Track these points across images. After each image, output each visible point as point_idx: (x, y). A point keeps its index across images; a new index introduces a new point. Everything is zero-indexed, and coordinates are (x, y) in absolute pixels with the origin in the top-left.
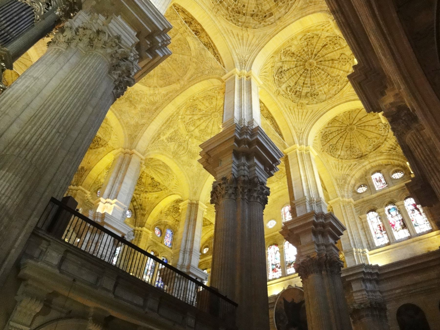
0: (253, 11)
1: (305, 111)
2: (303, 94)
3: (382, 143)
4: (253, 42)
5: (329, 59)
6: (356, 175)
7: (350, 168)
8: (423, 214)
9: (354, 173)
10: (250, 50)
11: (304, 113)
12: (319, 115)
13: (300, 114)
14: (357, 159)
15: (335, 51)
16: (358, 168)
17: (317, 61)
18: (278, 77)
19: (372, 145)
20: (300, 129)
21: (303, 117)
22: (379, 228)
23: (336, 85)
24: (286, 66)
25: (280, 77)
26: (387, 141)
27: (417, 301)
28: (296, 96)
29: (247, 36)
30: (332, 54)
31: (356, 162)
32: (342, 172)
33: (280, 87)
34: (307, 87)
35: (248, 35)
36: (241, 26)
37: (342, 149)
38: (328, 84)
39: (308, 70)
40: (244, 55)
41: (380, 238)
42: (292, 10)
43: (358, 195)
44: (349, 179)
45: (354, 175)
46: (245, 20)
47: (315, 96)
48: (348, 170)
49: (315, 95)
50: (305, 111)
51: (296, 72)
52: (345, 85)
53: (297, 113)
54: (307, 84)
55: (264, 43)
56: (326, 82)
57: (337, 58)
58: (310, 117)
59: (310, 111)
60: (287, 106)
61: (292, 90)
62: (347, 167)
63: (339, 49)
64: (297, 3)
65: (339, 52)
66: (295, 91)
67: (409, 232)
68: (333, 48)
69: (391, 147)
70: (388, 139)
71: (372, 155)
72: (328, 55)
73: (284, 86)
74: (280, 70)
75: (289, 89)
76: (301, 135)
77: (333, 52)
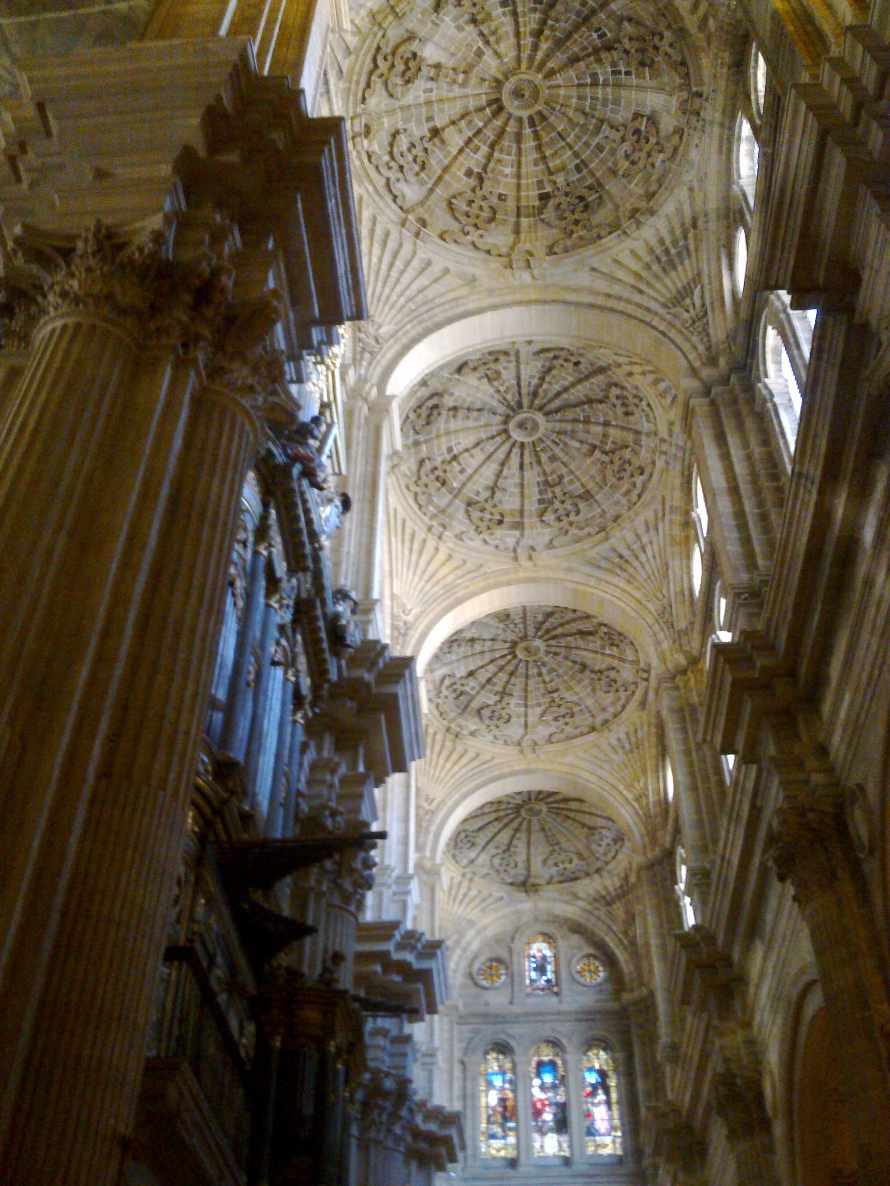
0: (478, 494)
2: (475, 705)
3: (588, 874)
4: (441, 574)
5: (578, 659)
7: (484, 905)
8: (615, 1107)
10: (426, 593)
11: (454, 757)
12: (488, 776)
13: (445, 753)
15: (603, 654)
21: (449, 765)
23: (562, 721)
26: (601, 876)
29: (432, 551)
30: (591, 655)
31: (503, 894)
32: (460, 912)
34: (491, 691)
36: (431, 518)
37: (484, 848)
38: (543, 707)
39: (515, 656)
40: (409, 607)
43: (478, 990)
45: (485, 928)
46: (449, 504)
47: (500, 723)
50: (460, 749)
52: (582, 734)
54: (495, 684)
55: (466, 591)
56: (541, 701)
57: (597, 668)
58: (464, 771)
59: (471, 754)
62: (477, 901)
63: (613, 657)
65: (609, 661)
67: (571, 1147)
68: (603, 647)
69: (604, 893)
70: (605, 873)
71: (550, 892)
72: (582, 653)
75: (447, 682)
76: (427, 817)
77: (596, 652)
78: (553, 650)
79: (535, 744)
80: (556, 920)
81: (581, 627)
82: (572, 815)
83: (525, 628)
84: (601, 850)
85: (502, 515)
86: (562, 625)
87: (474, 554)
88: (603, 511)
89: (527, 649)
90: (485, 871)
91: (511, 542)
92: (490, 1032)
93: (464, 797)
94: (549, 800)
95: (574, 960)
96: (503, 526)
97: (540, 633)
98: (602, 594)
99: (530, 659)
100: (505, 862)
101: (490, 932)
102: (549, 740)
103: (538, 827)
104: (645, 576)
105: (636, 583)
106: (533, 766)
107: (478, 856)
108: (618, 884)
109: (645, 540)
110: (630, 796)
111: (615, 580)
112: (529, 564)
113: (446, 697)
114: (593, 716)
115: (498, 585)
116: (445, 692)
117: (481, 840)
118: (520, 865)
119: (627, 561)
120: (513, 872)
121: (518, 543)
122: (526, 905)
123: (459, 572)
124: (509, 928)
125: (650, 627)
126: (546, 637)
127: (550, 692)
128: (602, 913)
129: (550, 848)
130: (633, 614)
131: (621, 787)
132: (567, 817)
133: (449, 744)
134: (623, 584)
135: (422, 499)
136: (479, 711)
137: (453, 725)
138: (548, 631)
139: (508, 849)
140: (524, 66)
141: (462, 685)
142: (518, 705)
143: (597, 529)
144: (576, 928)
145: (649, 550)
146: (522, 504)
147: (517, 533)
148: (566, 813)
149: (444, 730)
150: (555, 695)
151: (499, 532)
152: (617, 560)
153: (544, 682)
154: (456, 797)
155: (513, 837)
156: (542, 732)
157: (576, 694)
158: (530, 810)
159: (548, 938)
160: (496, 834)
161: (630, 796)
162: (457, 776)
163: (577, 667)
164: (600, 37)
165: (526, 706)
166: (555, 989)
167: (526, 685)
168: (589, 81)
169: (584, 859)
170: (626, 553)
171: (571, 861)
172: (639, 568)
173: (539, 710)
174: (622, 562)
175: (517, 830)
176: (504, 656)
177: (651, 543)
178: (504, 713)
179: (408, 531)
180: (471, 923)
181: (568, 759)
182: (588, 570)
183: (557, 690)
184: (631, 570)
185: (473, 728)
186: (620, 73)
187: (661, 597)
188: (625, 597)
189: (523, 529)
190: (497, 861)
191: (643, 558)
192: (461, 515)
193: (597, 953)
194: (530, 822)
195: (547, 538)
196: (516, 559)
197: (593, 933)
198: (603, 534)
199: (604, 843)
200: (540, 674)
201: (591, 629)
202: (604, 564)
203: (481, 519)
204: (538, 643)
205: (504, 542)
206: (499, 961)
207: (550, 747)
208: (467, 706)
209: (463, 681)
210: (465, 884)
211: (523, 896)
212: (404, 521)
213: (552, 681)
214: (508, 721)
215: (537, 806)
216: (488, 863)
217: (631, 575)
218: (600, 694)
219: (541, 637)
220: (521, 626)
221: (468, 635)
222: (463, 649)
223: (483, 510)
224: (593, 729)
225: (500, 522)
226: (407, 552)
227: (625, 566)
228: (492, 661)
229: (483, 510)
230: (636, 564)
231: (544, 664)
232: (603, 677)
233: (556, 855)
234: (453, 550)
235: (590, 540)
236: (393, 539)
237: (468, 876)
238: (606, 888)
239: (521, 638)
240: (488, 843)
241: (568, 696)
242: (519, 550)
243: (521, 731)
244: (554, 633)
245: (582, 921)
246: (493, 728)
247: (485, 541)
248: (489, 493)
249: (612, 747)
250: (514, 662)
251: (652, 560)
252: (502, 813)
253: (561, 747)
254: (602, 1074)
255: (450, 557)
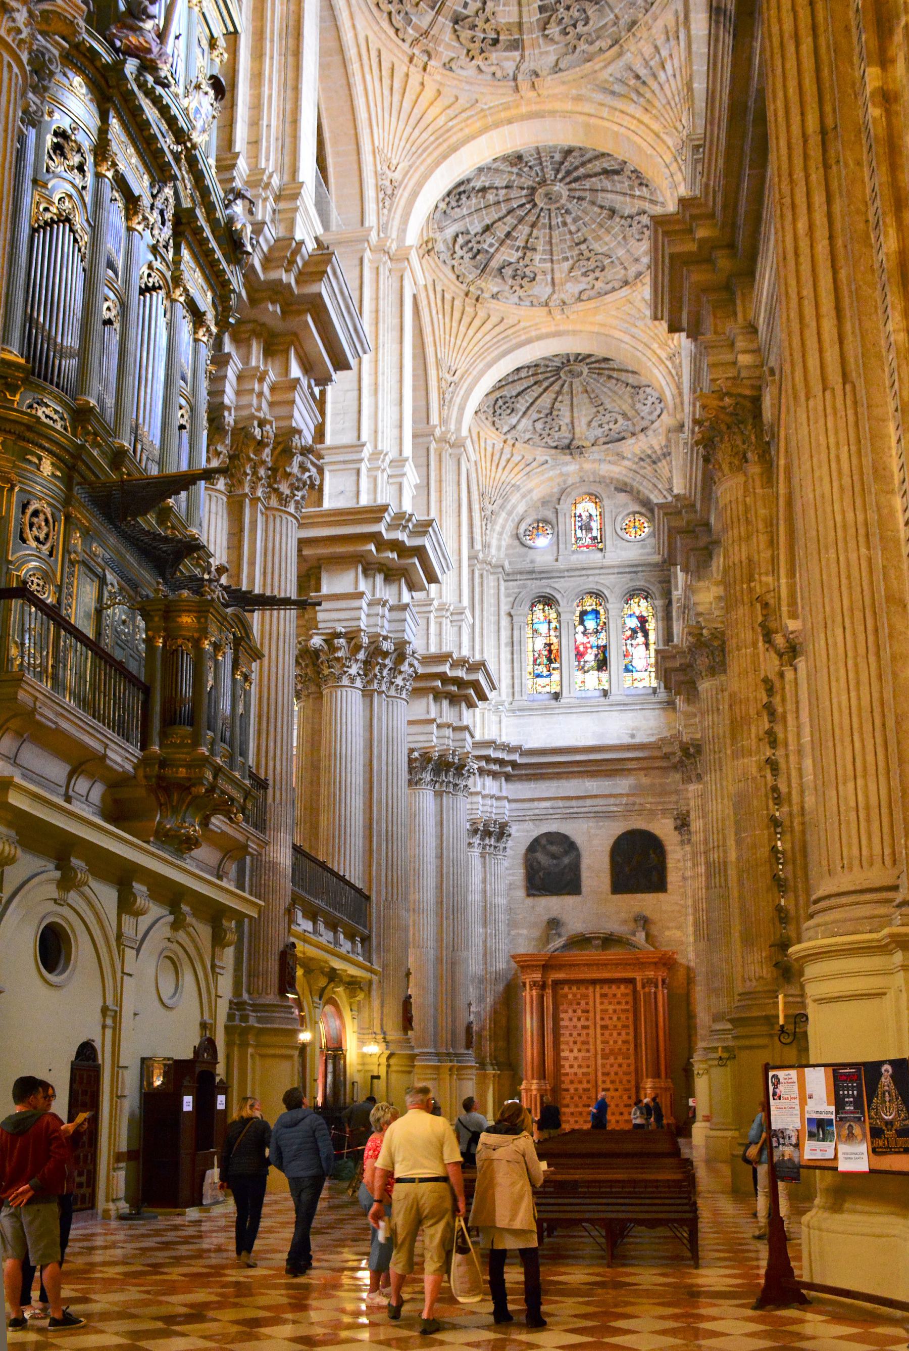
1: (482, 314)
2: (494, 264)
3: (633, 434)
5: (607, 204)
6: (535, 492)
9: (531, 485)
11: (477, 323)
12: (514, 342)
14: (553, 451)
15: (633, 196)
16: (546, 476)
17: (572, 194)
18: (448, 204)
19: (606, 427)
20: (453, 369)
21: (471, 332)
22: (546, 653)
23: (592, 276)
24: (483, 178)
25: (454, 204)
27: (573, 829)
28: (472, 262)
30: (620, 198)
33: (441, 229)
34: (512, 247)
35: (422, 84)
37: (525, 413)
38: (571, 262)
39: (535, 205)
40: (394, 162)
41: (542, 676)
42: (580, 74)
44: (514, 499)
45: (530, 491)
47: (524, 282)
48: (519, 476)
49: (526, 279)
50: (482, 314)
51: (501, 199)
52: (614, 290)
53: (457, 315)
55: (460, 135)
56: (569, 254)
58: (488, 338)
59: (494, 320)
60: (439, 289)
61: (470, 245)
62: (522, 465)
64: (602, 64)
66: (475, 250)
68: (632, 188)
69: (649, 452)
70: (650, 432)
71: (595, 453)
73: (450, 232)
74: (462, 189)
75: (460, 240)
76: (451, 389)
77: (625, 194)
78: (577, 194)
79: (564, 303)
80: (600, 480)
81: (605, 165)
82: (615, 374)
83: (542, 170)
84: (647, 409)
85: (498, 33)
86: (583, 164)
87: (467, 87)
88: (617, 17)
89: (547, 195)
90: (528, 436)
91: (510, 67)
92: (536, 587)
93: (489, 366)
94: (588, 361)
95: (620, 518)
96: (499, 46)
97: (559, 176)
98: (616, 128)
99: (553, 207)
100: (548, 426)
101: (536, 495)
102: (579, 299)
103: (580, 389)
104: (664, 101)
105: (654, 112)
106: (561, 328)
107: (519, 421)
108: (663, 443)
109: (664, 53)
111: (631, 109)
112: (533, 94)
113: (462, 258)
114: (625, 268)
115: (497, 125)
116: (459, 253)
117: (521, 405)
118: (563, 428)
119: (644, 83)
120: (556, 435)
121: (518, 68)
122: (571, 467)
123: (451, 112)
124: (555, 490)
125: (667, 166)
126: (568, 180)
127: (577, 244)
128: (648, 470)
129: (595, 410)
130: (650, 151)
131: (655, 346)
132: (610, 377)
133: (469, 310)
134: (639, 113)
135: (398, 20)
136: (500, 270)
137: (472, 289)
138: (568, 173)
139: (551, 413)
141: (479, 242)
142: (542, 261)
143: (610, 42)
144: (623, 488)
145: (668, 67)
146: (521, 17)
147: (516, 54)
148: (606, 372)
149: (462, 294)
150: (583, 247)
151: (494, 56)
152: (632, 82)
153: (570, 233)
154: (481, 366)
155: (556, 399)
156: (573, 288)
158: (570, 371)
159: (595, 498)
160: (537, 399)
161: (663, 355)
162: (481, 344)
163: (605, 212)
165: (552, 261)
166: (600, 546)
167: (551, 237)
169: (629, 419)
170: (642, 72)
171: (616, 422)
172: (658, 91)
173: (566, 265)
174: (638, 83)
175: (559, 393)
176: (522, 205)
177: (671, 55)
178: (527, 270)
179: (386, 65)
180: (516, 487)
181: (600, 318)
182: (599, 97)
183: (585, 240)
184: (648, 95)
185: (495, 290)
187: (680, 128)
188: (642, 130)
189: (523, 50)
190: (539, 425)
191: (662, 76)
192: (448, 36)
193: (643, 510)
194: (571, 384)
195: (552, 58)
196: (517, 89)
197: (638, 492)
198: (616, 47)
199: (649, 402)
200: (565, 224)
201: (616, 167)
202: (617, 88)
204: (559, 188)
205: (502, 69)
206: (546, 521)
207: (581, 306)
208: (486, 266)
209: (478, 238)
210: (508, 450)
211: (568, 458)
212: (379, 51)
213: (578, 230)
214: (534, 279)
215: (577, 368)
216: (531, 428)
217: (648, 101)
218: (632, 242)
219: (561, 180)
220: (537, 168)
221: (478, 185)
222: (474, 201)
223: (473, 27)
224: (626, 283)
225: (496, 42)
226: (386, 92)
227: (642, 89)
228: (509, 213)
229: (473, 27)
230: (655, 86)
231: (568, 212)
232: (635, 223)
233: (600, 416)
234: (441, 84)
235: (602, 57)
236: (368, 77)
237: (510, 442)
238: (652, 447)
239: (539, 183)
240: (528, 408)
241: (597, 247)
242: (520, 77)
243: (549, 290)
244: (575, 174)
245: (628, 480)
246: (517, 288)
250: (536, 211)
251: (671, 79)
252: (541, 377)
253: (591, 305)
254: (643, 620)
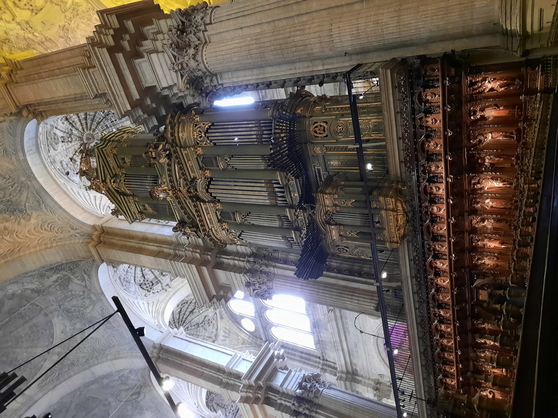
58: (193, 389)
68: (199, 312)
72: (195, 320)
85: (152, 282)
91: (160, 288)
110: (241, 346)
112: (171, 289)
114: (211, 338)
140: (85, 130)
146: (154, 275)
147: (159, 284)
157: (201, 335)
161: (241, 346)
164: (103, 113)
168: (105, 128)
186: (113, 121)
189: (160, 282)
203: (147, 287)
225: (153, 284)
229: (145, 284)
233: (227, 410)
247: (153, 293)
248: (143, 279)
249: (223, 340)
255: (148, 303)
